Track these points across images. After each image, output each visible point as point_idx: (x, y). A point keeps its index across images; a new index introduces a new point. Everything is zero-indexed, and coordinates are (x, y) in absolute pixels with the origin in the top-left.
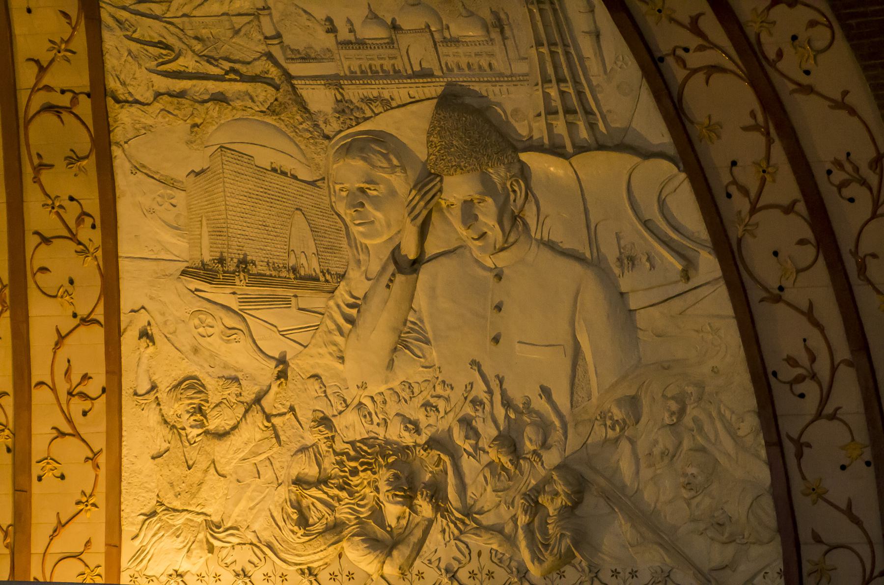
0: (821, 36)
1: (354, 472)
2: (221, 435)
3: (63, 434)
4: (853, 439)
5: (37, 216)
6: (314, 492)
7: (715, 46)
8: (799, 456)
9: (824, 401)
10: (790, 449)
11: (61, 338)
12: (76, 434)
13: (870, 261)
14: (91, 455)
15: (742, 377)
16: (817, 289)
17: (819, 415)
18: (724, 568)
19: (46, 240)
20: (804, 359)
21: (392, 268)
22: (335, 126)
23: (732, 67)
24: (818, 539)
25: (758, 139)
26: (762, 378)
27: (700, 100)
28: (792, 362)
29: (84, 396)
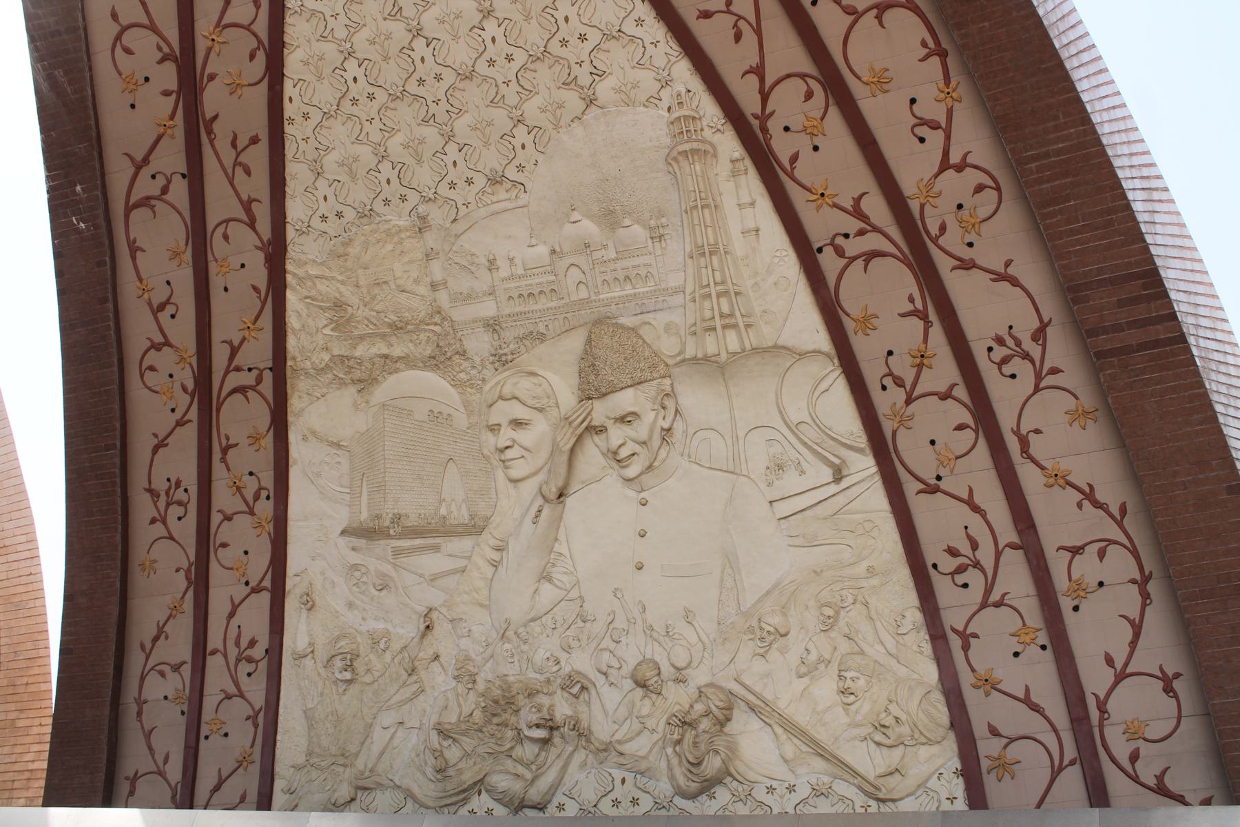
3: (229, 697)
4: (1024, 625)
7: (876, 229)
8: (966, 647)
9: (988, 591)
10: (955, 642)
12: (242, 696)
13: (1032, 438)
14: (252, 713)
15: (904, 574)
17: (984, 605)
18: (891, 774)
20: (965, 548)
21: (540, 501)
23: (891, 249)
24: (994, 732)
27: (855, 292)
28: (953, 552)
29: (250, 660)
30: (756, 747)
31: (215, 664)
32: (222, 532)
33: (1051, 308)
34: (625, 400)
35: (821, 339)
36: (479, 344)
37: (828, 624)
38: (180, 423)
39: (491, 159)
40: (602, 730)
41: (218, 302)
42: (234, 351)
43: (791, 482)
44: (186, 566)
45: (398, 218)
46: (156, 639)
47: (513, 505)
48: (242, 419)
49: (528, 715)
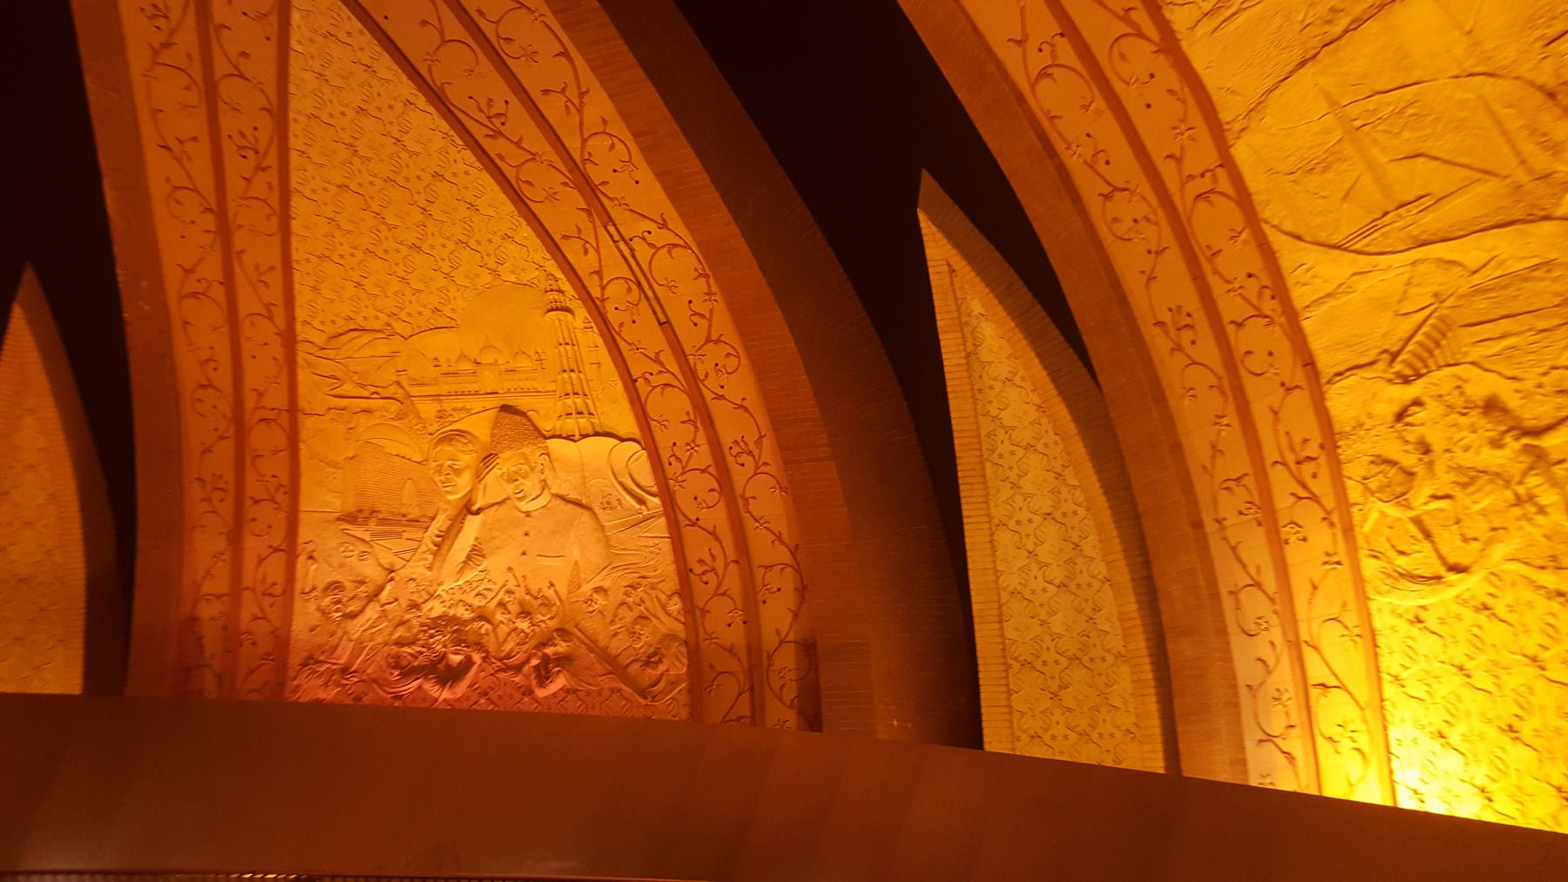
0: (732, 363)
1: (432, 636)
2: (353, 616)
5: (253, 488)
6: (407, 649)
9: (718, 587)
10: (698, 613)
11: (261, 560)
16: (717, 517)
19: (257, 502)
20: (709, 560)
22: (435, 427)
23: (675, 383)
24: (711, 666)
25: (689, 428)
26: (684, 572)
28: (701, 561)
29: (271, 595)
32: (252, 511)
38: (221, 438)
41: (248, 365)
42: (261, 395)
44: (225, 530)
46: (205, 577)
48: (264, 439)
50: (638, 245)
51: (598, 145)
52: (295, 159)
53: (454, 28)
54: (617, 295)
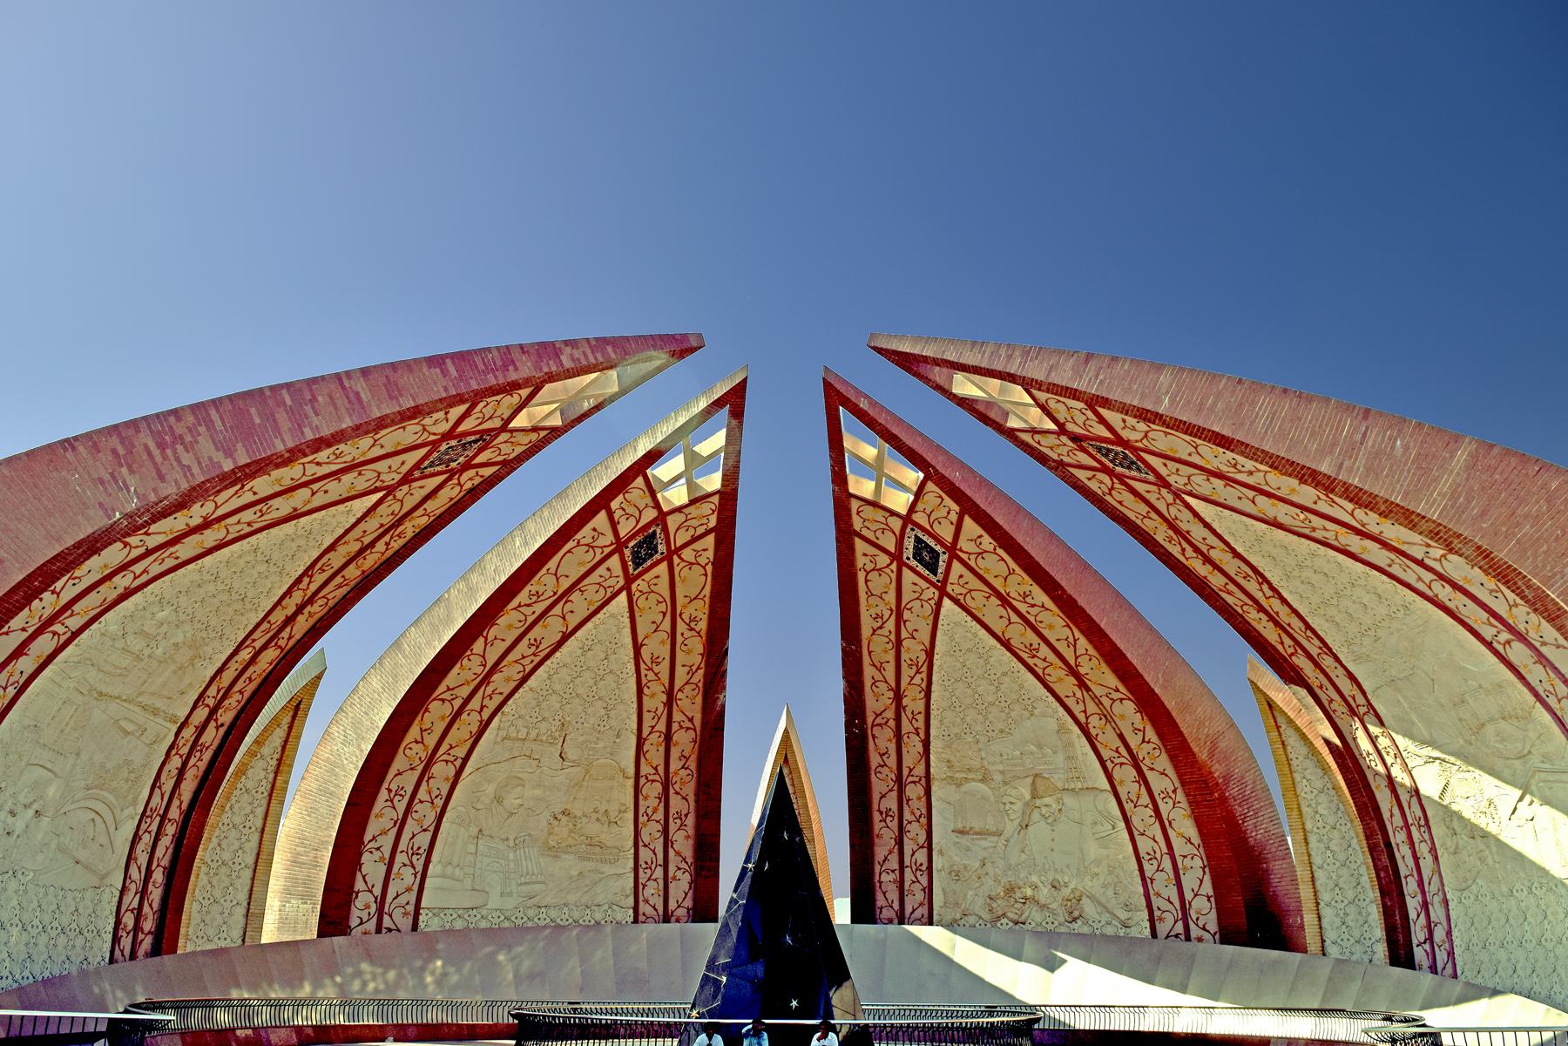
0: (1157, 752)
27: (1117, 774)
30: (1089, 908)
31: (907, 871)
32: (909, 827)
33: (1177, 784)
34: (1047, 800)
35: (1108, 787)
36: (998, 777)
37: (1111, 873)
39: (1001, 726)
40: (1043, 901)
43: (1099, 828)
45: (969, 739)
47: (1010, 828)
48: (914, 791)
49: (1018, 895)
50: (1104, 700)
51: (1083, 660)
52: (935, 668)
53: (1014, 618)
54: (1095, 723)
